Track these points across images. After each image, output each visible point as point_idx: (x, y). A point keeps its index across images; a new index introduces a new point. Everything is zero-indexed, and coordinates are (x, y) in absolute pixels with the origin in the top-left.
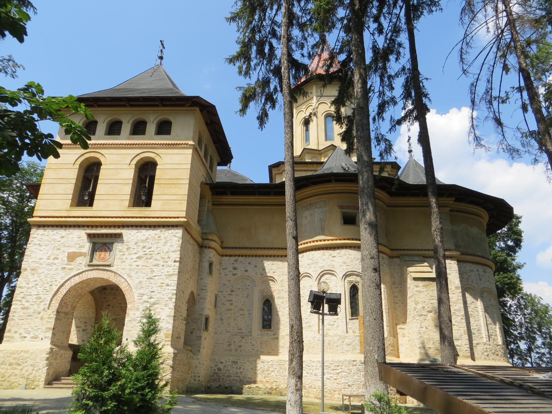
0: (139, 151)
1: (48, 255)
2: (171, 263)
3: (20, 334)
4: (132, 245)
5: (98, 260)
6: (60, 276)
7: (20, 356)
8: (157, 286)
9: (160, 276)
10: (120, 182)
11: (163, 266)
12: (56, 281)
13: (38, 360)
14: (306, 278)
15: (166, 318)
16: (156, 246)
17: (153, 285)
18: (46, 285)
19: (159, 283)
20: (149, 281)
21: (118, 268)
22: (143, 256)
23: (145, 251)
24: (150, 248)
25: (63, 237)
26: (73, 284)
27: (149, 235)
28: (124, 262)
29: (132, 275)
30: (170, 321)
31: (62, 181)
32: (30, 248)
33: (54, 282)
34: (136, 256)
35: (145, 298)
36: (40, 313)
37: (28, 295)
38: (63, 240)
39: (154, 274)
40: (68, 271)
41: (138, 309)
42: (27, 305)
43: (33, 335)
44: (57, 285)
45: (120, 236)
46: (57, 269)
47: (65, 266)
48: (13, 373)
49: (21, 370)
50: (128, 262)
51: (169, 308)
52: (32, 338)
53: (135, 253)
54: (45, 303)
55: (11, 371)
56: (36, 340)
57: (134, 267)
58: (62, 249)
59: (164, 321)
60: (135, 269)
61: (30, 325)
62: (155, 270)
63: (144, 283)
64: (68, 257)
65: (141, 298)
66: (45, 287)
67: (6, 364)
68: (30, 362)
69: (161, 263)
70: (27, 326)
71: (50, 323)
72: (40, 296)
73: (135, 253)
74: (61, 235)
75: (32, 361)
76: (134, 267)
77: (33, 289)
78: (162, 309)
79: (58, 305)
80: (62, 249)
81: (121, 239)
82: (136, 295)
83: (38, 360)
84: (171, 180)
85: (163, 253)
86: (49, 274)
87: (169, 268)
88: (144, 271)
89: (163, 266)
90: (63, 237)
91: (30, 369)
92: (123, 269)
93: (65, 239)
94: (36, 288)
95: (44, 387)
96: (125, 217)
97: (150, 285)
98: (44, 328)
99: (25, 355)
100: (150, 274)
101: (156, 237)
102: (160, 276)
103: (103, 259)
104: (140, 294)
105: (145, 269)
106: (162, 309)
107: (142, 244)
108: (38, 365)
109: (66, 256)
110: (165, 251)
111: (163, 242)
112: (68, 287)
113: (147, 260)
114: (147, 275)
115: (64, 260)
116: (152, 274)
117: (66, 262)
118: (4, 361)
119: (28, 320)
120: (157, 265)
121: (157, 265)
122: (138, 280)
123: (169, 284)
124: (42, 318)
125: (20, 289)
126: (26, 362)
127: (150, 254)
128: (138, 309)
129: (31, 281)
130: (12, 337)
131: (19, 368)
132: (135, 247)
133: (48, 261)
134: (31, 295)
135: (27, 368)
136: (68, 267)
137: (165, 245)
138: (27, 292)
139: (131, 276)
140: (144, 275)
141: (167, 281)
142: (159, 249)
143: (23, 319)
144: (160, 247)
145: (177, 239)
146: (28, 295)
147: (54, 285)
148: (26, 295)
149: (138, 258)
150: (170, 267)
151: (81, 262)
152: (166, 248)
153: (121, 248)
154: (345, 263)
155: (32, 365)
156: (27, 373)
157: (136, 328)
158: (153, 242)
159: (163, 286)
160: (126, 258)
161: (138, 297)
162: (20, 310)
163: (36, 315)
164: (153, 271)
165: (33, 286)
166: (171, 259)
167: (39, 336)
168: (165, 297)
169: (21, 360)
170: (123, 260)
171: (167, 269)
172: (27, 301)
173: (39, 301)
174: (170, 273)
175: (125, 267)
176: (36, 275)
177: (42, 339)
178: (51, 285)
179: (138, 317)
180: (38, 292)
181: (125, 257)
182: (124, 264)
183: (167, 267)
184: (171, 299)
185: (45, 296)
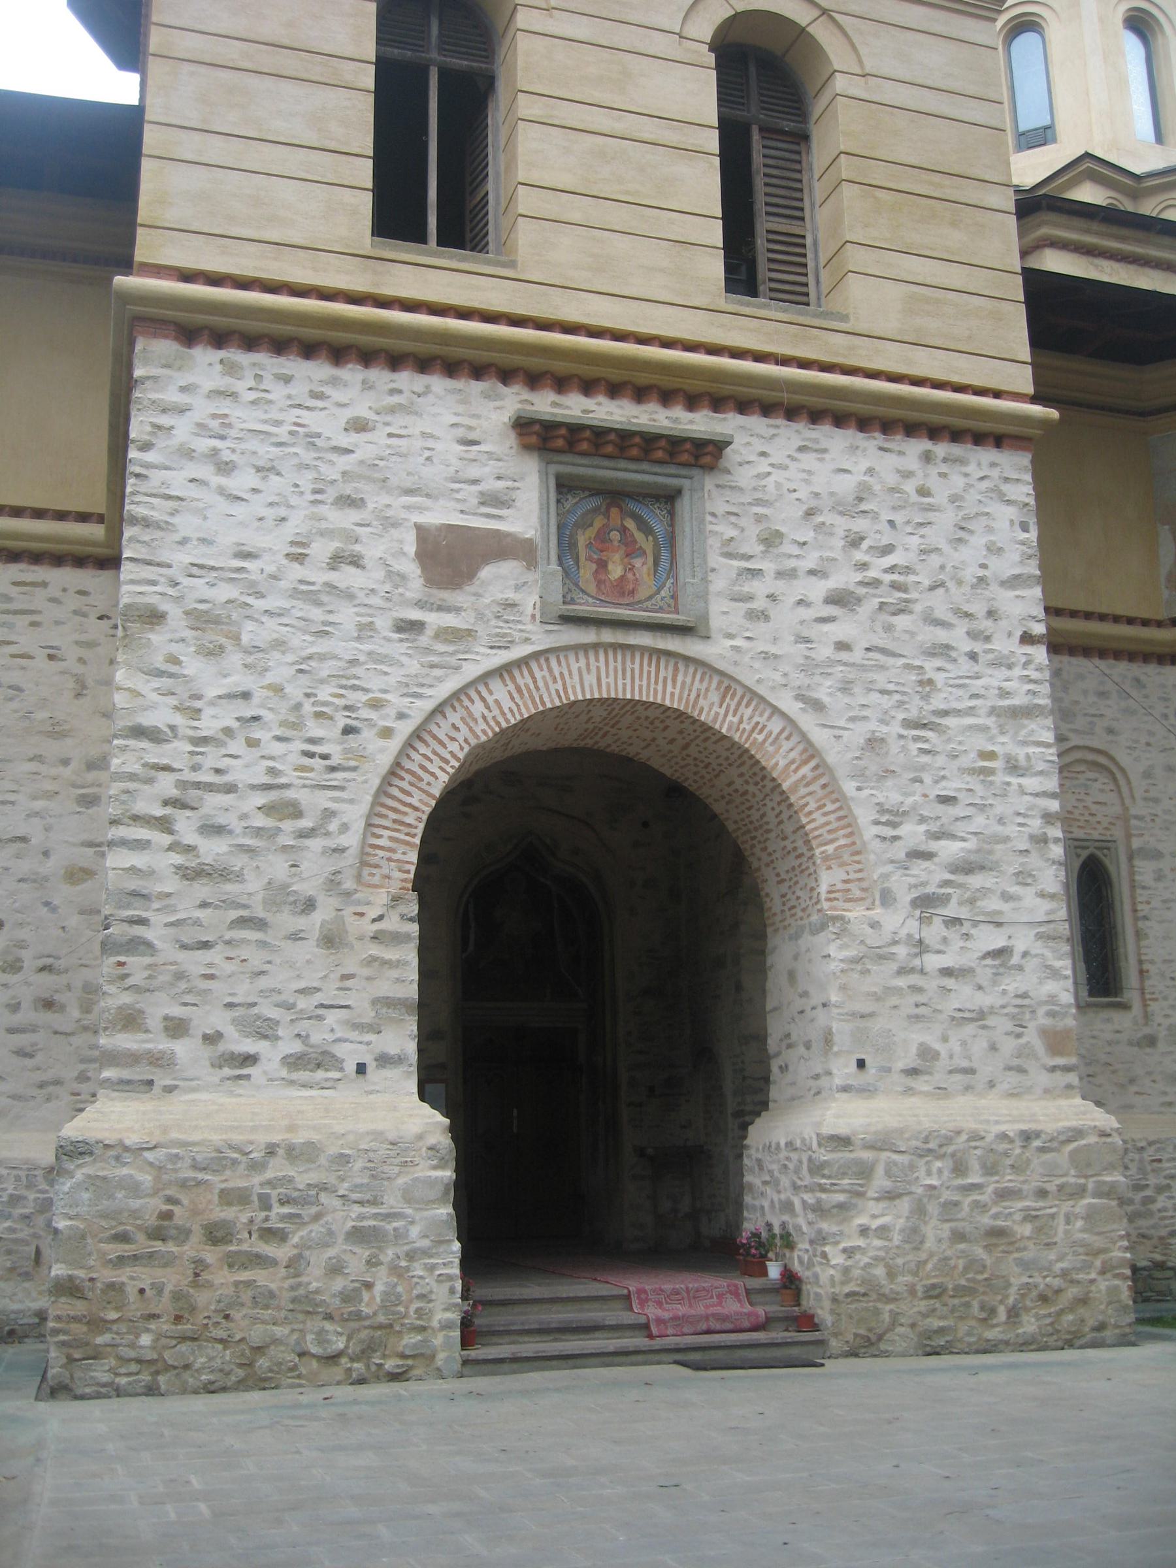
1: (290, 530)
3: (212, 1039)
5: (592, 588)
6: (396, 675)
7: (269, 1183)
8: (963, 771)
9: (971, 711)
10: (649, 129)
11: (973, 656)
12: (376, 705)
13: (392, 1201)
15: (1038, 948)
16: (915, 541)
17: (940, 761)
18: (315, 729)
19: (973, 755)
20: (917, 739)
21: (735, 649)
22: (862, 591)
23: (864, 566)
24: (888, 550)
25: (359, 426)
26: (484, 732)
27: (870, 471)
28: (764, 616)
29: (822, 694)
30: (1058, 964)
31: (289, 63)
32: (156, 477)
33: (364, 713)
34: (817, 589)
35: (912, 833)
36: (309, 905)
37: (210, 787)
38: (367, 447)
39: (937, 703)
40: (441, 647)
41: (887, 898)
42: (212, 850)
43: (296, 1047)
44: (387, 733)
46: (365, 630)
47: (415, 615)
48: (249, 1284)
49: (295, 1264)
50: (786, 617)
51: (1042, 895)
52: (295, 1062)
53: (812, 572)
54: (331, 843)
55: (223, 1278)
56: (320, 1074)
57: (825, 651)
58: (376, 500)
59: (1031, 964)
60: (832, 663)
61: (263, 983)
62: (939, 678)
63: (894, 747)
65: (889, 832)
66: (312, 741)
67: (184, 1234)
68: (343, 1218)
69: (957, 637)
70: (243, 991)
71: (394, 974)
72: (290, 794)
73: (812, 572)
74: (348, 413)
75: (357, 1209)
76: (825, 651)
77: (236, 746)
78: (1006, 897)
79: (413, 857)
80: (376, 500)
81: (723, 479)
82: (864, 816)
83: (392, 1201)
84: (925, 176)
85: (960, 583)
86: (322, 657)
87: (1004, 672)
88: (881, 679)
89: (973, 656)
90: (359, 426)
91: (356, 1260)
92: (766, 656)
93: (379, 436)
94: (252, 743)
95: (466, 1362)
97: (925, 759)
98: (360, 1000)
99: (304, 1177)
100: (917, 701)
101: (910, 487)
102: (971, 711)
103: (623, 590)
104: (882, 810)
105: (882, 668)
106: (1006, 897)
107: (841, 524)
108: (399, 1235)
109: (411, 549)
110: (971, 573)
111: (947, 519)
112: (454, 747)
113: (885, 617)
114: (901, 704)
115: (403, 577)
116: (926, 698)
117: (416, 585)
118: (167, 1216)
119: (244, 953)
120: (943, 650)
121: (943, 650)
122: (861, 731)
123: (1022, 761)
124: (331, 940)
125: (145, 744)
126: (317, 1217)
127: (895, 586)
128: (887, 898)
129: (212, 692)
130: (159, 1060)
131: (281, 1252)
132: (808, 535)
133: (297, 572)
134: (230, 789)
135: (331, 1252)
136: (434, 619)
137: (960, 540)
138: (195, 768)
139: (817, 706)
140: (886, 702)
141: (1004, 745)
142: (935, 560)
143: (205, 945)
144: (937, 550)
145: (1011, 512)
146: (210, 787)
147: (367, 734)
148: (198, 785)
149: (839, 599)
150: (1010, 667)
151: (511, 595)
152: (970, 557)
153: (731, 533)
155: (358, 1235)
156: (339, 1284)
157: (894, 1001)
158: (899, 518)
159: (991, 772)
160: (772, 597)
161: (876, 830)
162: (171, 884)
163: (287, 920)
164: (930, 682)
165: (228, 731)
166: (1004, 624)
167: (340, 1050)
168: (1011, 830)
169: (282, 1203)
170: (754, 605)
171: (994, 679)
172: (214, 830)
173: (288, 825)
174: (1017, 701)
175: (773, 650)
176: (235, 659)
177: (361, 1069)
178: (348, 731)
179: (895, 943)
180: (272, 771)
181: (759, 588)
182: (761, 628)
183: (994, 664)
184: (1041, 840)
185: (323, 800)
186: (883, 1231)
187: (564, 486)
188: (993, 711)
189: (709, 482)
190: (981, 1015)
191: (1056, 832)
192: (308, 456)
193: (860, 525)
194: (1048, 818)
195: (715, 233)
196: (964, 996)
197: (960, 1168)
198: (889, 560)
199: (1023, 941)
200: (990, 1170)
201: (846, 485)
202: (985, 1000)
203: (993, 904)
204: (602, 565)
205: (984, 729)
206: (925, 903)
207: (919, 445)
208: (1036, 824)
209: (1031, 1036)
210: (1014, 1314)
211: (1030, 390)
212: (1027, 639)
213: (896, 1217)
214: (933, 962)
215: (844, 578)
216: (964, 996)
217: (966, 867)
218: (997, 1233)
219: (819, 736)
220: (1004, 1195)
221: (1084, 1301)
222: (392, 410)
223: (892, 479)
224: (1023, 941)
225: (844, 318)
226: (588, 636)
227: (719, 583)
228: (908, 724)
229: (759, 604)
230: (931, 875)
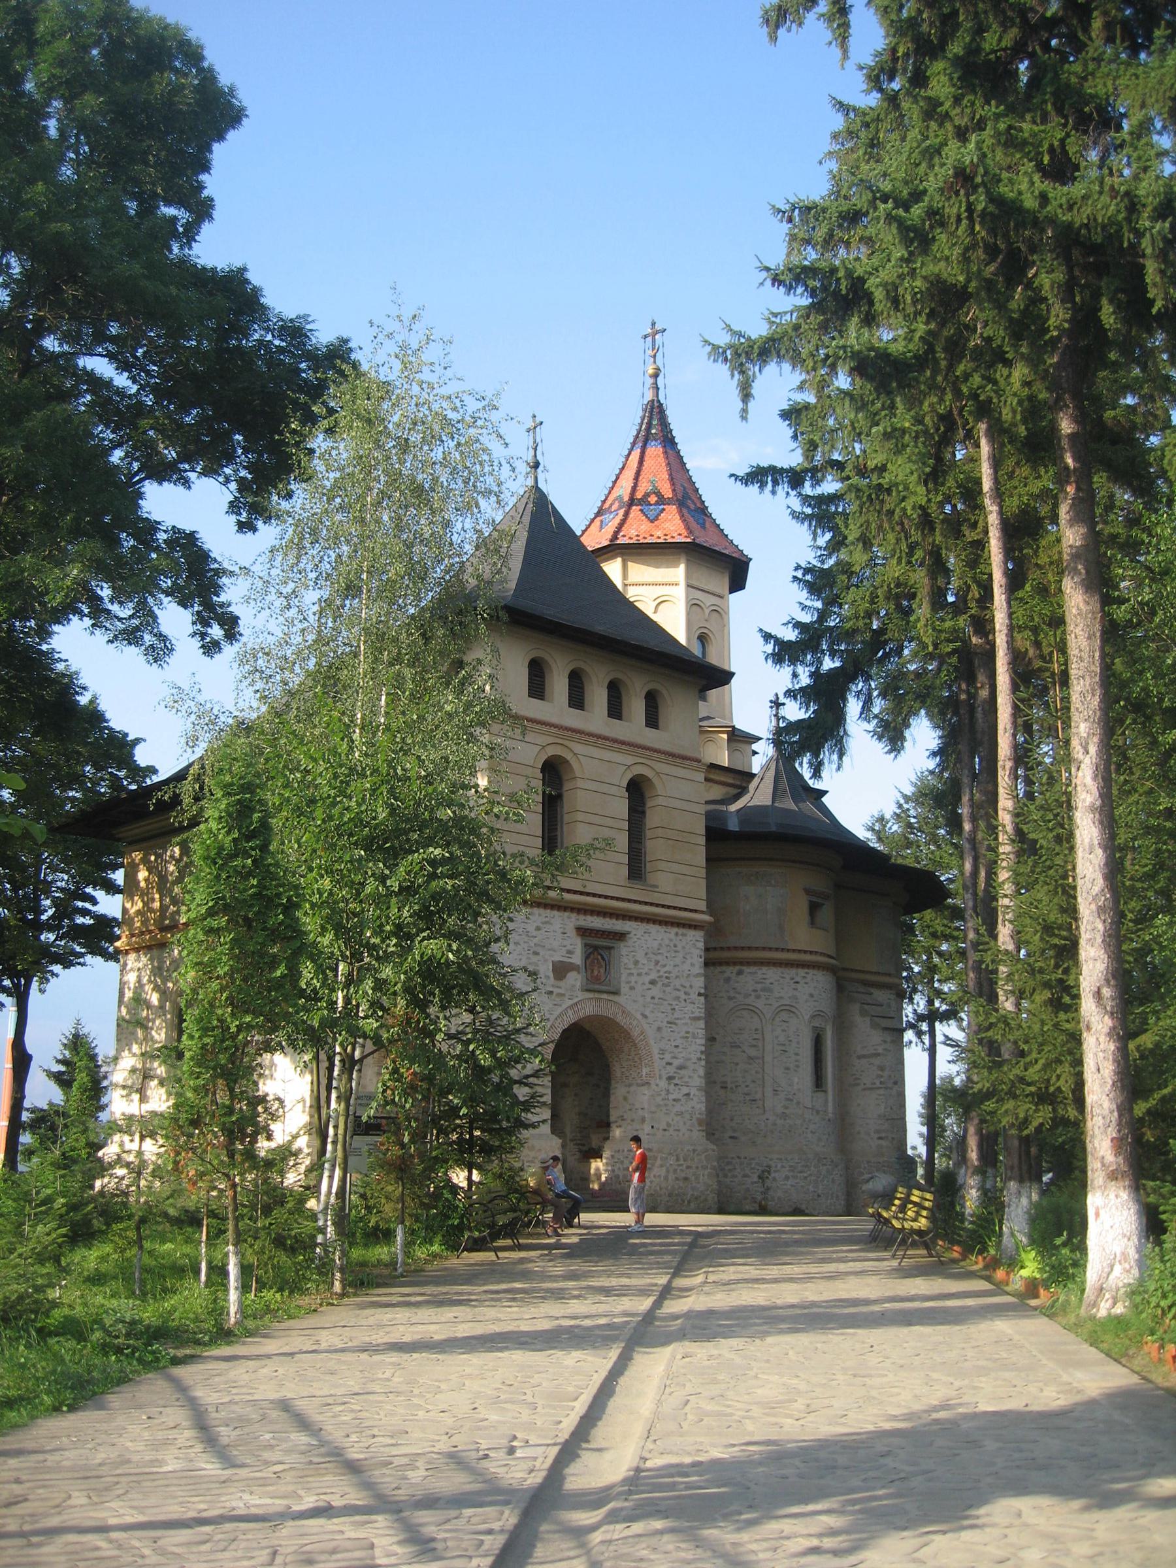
0: (630, 760)
2: (694, 996)
4: (640, 956)
14: (745, 1013)
24: (665, 966)
25: (538, 929)
29: (647, 1013)
34: (647, 979)
35: (668, 1057)
39: (676, 1016)
45: (621, 936)
57: (649, 999)
64: (554, 970)
80: (542, 953)
82: (655, 1051)
96: (618, 899)
107: (654, 958)
111: (681, 955)
120: (678, 998)
121: (678, 998)
136: (556, 991)
139: (645, 1016)
142: (677, 969)
149: (653, 982)
152: (686, 967)
154: (812, 996)
171: (690, 1007)
181: (633, 979)
184: (700, 1059)
186: (659, 1176)
187: (586, 945)
188: (690, 1018)
189: (622, 944)
190: (681, 1114)
191: (703, 1057)
192: (526, 939)
193: (659, 958)
194: (702, 1052)
195: (625, 859)
196: (678, 1108)
197: (678, 1160)
198: (666, 969)
199: (693, 1091)
200: (685, 1160)
201: (655, 944)
202: (683, 1109)
203: (686, 1079)
204: (592, 971)
205: (686, 1024)
206: (670, 1078)
207: (675, 930)
208: (699, 1055)
209: (694, 1120)
210: (689, 1202)
211: (704, 909)
212: (700, 994)
213: (663, 1172)
214: (671, 1097)
215: (653, 976)
216: (678, 1108)
217: (681, 1068)
218: (686, 1179)
219: (646, 1026)
220: (688, 1167)
221: (706, 1200)
222: (546, 923)
223: (667, 942)
224: (693, 1091)
225: (657, 887)
226: (591, 995)
227: (624, 978)
228: (669, 1023)
229: (633, 984)
230: (671, 1070)
